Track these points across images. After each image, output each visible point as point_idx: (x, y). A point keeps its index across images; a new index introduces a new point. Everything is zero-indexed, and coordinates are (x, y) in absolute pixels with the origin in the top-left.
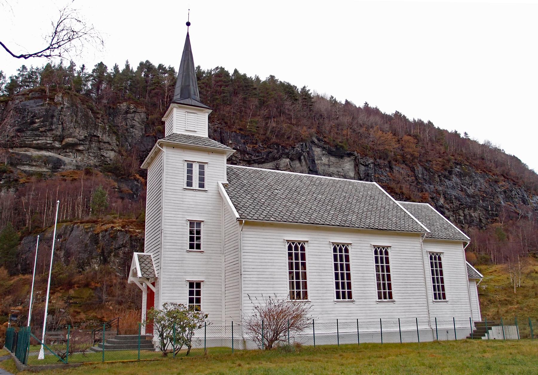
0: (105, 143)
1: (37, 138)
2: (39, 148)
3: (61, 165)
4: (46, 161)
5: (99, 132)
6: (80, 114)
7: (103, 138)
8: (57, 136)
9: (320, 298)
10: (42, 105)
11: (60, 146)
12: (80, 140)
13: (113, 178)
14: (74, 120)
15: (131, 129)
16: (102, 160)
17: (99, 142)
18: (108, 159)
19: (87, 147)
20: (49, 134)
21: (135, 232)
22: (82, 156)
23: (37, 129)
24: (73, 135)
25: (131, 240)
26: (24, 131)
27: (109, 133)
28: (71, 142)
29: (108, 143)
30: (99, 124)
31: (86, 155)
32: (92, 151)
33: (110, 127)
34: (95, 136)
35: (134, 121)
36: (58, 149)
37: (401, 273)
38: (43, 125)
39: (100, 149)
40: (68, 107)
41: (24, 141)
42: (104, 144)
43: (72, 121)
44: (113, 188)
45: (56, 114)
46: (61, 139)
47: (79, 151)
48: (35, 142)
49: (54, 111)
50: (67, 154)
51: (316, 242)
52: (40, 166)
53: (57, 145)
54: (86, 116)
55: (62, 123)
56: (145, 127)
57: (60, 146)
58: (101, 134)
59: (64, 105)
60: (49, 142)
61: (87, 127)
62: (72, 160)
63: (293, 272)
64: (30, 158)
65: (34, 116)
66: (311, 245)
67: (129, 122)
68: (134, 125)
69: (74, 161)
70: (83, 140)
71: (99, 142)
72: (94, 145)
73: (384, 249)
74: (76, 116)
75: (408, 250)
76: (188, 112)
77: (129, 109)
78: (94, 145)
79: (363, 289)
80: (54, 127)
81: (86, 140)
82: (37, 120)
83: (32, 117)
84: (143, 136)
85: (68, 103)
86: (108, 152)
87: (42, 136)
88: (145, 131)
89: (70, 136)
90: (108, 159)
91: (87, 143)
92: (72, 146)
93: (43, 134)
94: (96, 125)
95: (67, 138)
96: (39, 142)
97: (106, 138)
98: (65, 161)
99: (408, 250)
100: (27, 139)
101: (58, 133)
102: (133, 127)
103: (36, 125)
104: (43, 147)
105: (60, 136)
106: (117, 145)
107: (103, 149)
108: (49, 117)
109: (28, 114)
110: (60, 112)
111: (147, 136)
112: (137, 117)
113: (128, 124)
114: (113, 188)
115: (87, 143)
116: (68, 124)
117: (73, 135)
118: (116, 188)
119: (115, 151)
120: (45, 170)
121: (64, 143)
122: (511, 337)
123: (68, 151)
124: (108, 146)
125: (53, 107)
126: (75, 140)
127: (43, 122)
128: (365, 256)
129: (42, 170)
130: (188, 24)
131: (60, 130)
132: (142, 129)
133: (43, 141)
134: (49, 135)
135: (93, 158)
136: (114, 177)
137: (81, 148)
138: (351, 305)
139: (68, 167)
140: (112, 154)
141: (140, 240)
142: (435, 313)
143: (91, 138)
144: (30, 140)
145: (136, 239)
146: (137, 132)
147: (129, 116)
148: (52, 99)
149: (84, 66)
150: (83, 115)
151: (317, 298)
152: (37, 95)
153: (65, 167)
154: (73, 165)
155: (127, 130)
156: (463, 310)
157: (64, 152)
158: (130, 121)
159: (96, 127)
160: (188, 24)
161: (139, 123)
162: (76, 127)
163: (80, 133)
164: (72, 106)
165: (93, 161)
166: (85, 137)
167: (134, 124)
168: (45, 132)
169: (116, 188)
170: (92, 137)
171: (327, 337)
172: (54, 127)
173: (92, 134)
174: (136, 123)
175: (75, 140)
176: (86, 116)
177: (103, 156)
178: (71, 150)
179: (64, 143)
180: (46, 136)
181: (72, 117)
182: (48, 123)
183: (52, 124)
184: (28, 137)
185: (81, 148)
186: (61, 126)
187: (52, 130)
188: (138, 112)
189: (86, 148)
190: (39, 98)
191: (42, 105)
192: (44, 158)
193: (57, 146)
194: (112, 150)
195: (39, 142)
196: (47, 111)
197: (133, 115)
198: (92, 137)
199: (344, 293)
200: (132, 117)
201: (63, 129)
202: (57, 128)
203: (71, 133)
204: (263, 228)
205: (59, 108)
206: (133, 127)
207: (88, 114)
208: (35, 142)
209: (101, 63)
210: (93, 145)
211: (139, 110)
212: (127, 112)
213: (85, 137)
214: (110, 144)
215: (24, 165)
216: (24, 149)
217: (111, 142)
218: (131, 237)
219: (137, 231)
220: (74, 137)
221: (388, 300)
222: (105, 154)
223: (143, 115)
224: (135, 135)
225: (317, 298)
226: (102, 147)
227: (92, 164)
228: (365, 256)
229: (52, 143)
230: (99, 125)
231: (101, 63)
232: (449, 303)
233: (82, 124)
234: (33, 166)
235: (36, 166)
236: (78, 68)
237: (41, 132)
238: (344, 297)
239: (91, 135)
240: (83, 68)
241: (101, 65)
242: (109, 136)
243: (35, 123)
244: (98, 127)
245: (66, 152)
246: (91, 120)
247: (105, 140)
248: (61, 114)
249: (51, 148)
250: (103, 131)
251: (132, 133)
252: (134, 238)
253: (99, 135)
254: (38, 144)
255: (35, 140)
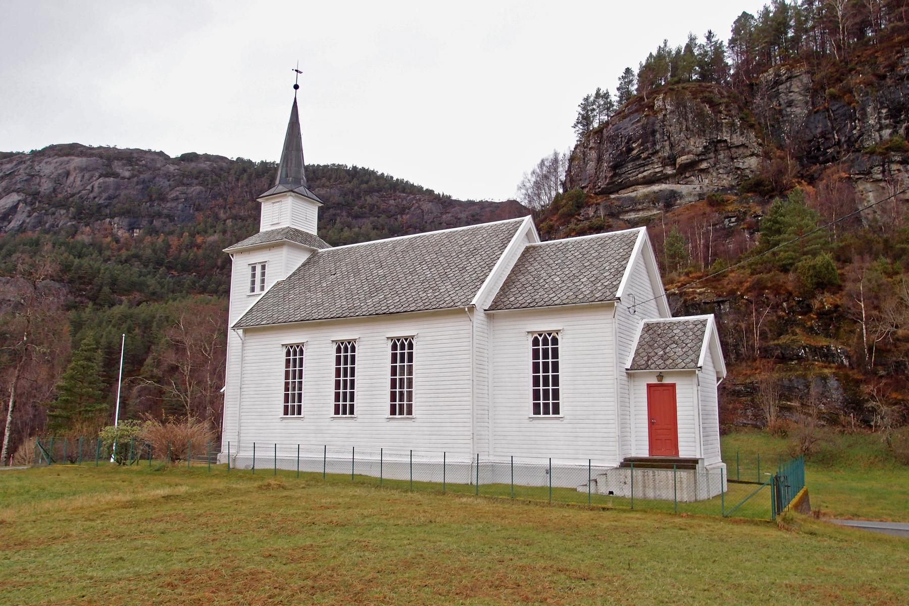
0: (737, 147)
1: (642, 169)
2: (649, 182)
3: (676, 200)
4: (654, 199)
5: (725, 134)
6: (690, 116)
7: (732, 141)
8: (664, 158)
9: (315, 413)
10: (638, 121)
11: (675, 171)
12: (698, 155)
13: (756, 200)
14: (684, 127)
15: (788, 109)
16: (739, 175)
17: (729, 148)
18: (748, 171)
19: (712, 161)
20: (655, 159)
21: (694, 292)
22: (710, 176)
23: (638, 157)
24: (687, 150)
25: (686, 307)
26: (622, 165)
27: (741, 131)
28: (685, 162)
29: (743, 145)
30: (723, 121)
31: (714, 174)
32: (722, 165)
33: (741, 119)
34: (720, 141)
35: (792, 94)
36: (673, 176)
37: (430, 375)
38: (643, 149)
39: (732, 159)
40: (672, 112)
41: (627, 178)
42: (737, 150)
43: (681, 131)
44: (755, 217)
45: (657, 127)
46: (671, 161)
47: (702, 171)
48: (640, 176)
49: (653, 124)
50: (688, 179)
51: (315, 343)
52: (648, 209)
53: (669, 171)
54: (700, 115)
55: (669, 137)
56: (812, 97)
57: (675, 171)
58: (729, 135)
59: (666, 109)
60: (657, 170)
61: (704, 132)
62: (695, 186)
63: (400, 375)
64: (633, 201)
65: (630, 140)
66: (422, 339)
67: (783, 98)
68: (793, 101)
69: (698, 189)
70: (702, 154)
71: (729, 148)
72: (722, 155)
73: (406, 340)
74: (687, 120)
75: (448, 337)
76: (273, 203)
77: (780, 76)
78: (722, 155)
79: (370, 401)
80: (658, 147)
81: (709, 151)
82: (634, 145)
83: (627, 143)
84: (809, 115)
85: (671, 105)
86: (745, 160)
87: (647, 165)
88: (813, 104)
89: (683, 153)
90: (748, 171)
91: (712, 155)
92: (690, 166)
93: (647, 162)
94: (717, 124)
95: (680, 157)
96: (645, 174)
97: (737, 139)
98: (681, 192)
99: (448, 337)
100: (630, 174)
101: (666, 154)
102: (790, 104)
103: (635, 152)
104: (653, 179)
105: (669, 158)
106: (760, 145)
107: (736, 158)
108: (648, 134)
109: (621, 140)
110: (663, 122)
111: (816, 112)
112: (796, 86)
113: (782, 102)
114: (755, 217)
115: (712, 155)
116: (675, 137)
117: (687, 150)
118: (760, 216)
119: (757, 156)
120: (655, 212)
121: (677, 166)
122: (658, 493)
123: (687, 175)
124: (745, 151)
125: (652, 119)
126: (691, 156)
127: (642, 144)
128: (378, 354)
129: (650, 213)
130: (296, 87)
131: (668, 148)
132: (807, 103)
133: (649, 172)
134: (656, 160)
135: (725, 176)
136: (758, 199)
137: (704, 165)
138: (351, 423)
139: (688, 199)
140: (753, 162)
141: (699, 305)
142: (533, 438)
143: (716, 146)
144: (634, 174)
145: (693, 305)
146: (798, 110)
147: (782, 88)
148: (651, 107)
149: (710, 32)
150: (695, 116)
151: (312, 413)
152: (634, 108)
153: (683, 201)
154: (695, 195)
155: (780, 111)
156: (597, 435)
157: (683, 179)
158: (784, 97)
159: (718, 127)
160: (296, 87)
161: (800, 94)
162: (689, 136)
163: (697, 144)
164: (678, 108)
165: (727, 180)
166: (705, 147)
167: (791, 98)
168: (650, 158)
169: (760, 216)
170: (715, 146)
171: (314, 462)
172: (658, 147)
173: (715, 140)
174: (793, 96)
175: (691, 157)
176: (700, 115)
177: (738, 169)
178: (691, 173)
179: (677, 166)
180: (652, 163)
181: (681, 123)
182: (649, 145)
183: (654, 144)
184: (630, 172)
185: (704, 165)
186: (667, 143)
187: (657, 152)
188: (796, 76)
189: (712, 163)
190: (637, 111)
191: (638, 121)
192: (652, 196)
193: (670, 172)
194: (752, 155)
195: (645, 174)
196: (644, 127)
197: (788, 84)
198: (715, 146)
199: (345, 406)
200: (787, 88)
201: (672, 146)
202: (663, 147)
203: (683, 148)
204: (264, 333)
205: (660, 117)
206: (790, 104)
207: (702, 110)
208: (640, 176)
209: (744, 13)
210: (721, 156)
211: (796, 72)
212: (777, 83)
213: (705, 147)
214: (747, 147)
215: (627, 212)
216: (631, 189)
217: (747, 143)
218: (685, 301)
219: (698, 291)
220: (689, 153)
221: (551, 415)
222: (741, 165)
223: (805, 79)
224: (796, 116)
225: (312, 413)
226: (734, 156)
227: (726, 186)
228: (378, 354)
229: (662, 171)
230: (722, 123)
231: (744, 13)
232: (565, 421)
233: (695, 130)
234: (639, 210)
235: (643, 209)
236: (701, 40)
237: (645, 159)
238: (401, 413)
239: (713, 142)
240: (710, 36)
241: (745, 15)
242: (742, 134)
243: (633, 149)
244: (722, 127)
245: (686, 177)
246: (708, 119)
247: (737, 143)
248: (665, 125)
249: (663, 179)
250: (731, 130)
251: (791, 114)
252: (690, 303)
253: (725, 138)
254: (644, 177)
255: (640, 173)
